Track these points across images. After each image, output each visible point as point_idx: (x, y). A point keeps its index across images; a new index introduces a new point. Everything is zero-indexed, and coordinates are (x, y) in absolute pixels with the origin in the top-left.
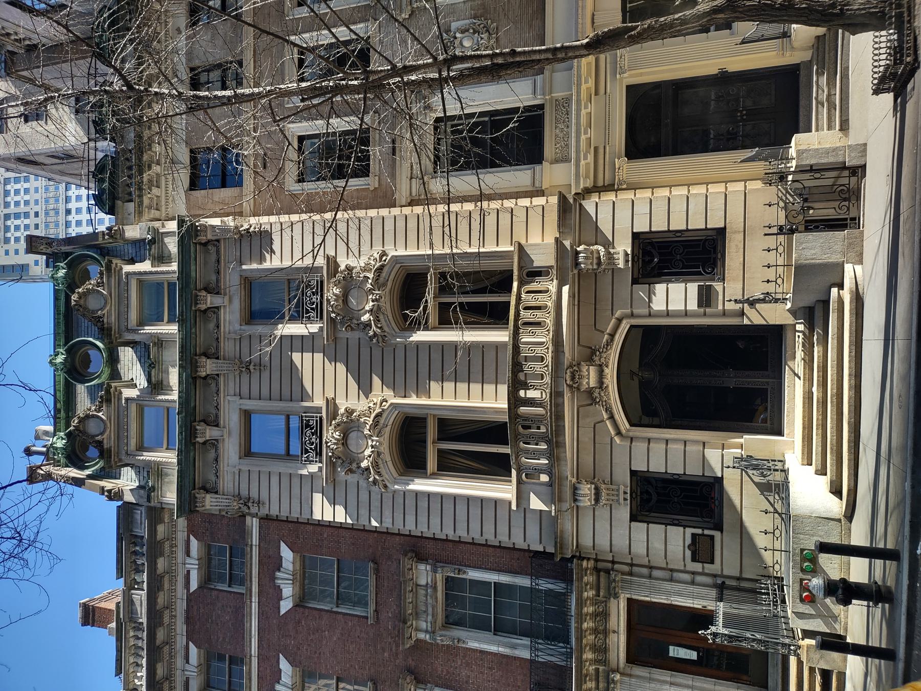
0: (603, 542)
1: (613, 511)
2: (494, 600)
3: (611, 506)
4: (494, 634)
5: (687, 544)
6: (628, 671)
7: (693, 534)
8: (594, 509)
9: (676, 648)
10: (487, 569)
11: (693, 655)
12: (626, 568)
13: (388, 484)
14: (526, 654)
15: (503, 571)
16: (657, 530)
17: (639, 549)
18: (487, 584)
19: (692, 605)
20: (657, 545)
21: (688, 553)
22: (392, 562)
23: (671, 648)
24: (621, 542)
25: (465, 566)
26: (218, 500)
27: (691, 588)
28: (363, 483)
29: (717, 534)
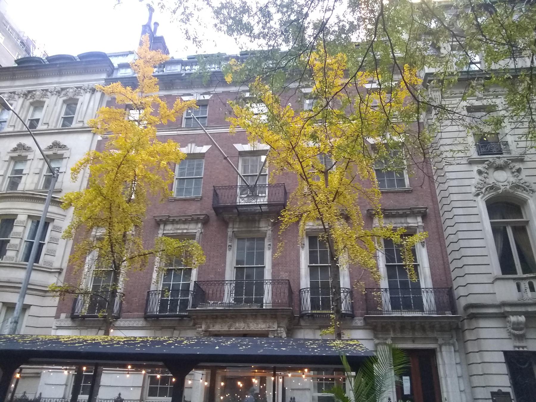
0: (483, 333)
5: (500, 388)
8: (506, 327)
9: (409, 381)
10: (429, 259)
11: (407, 391)
12: (457, 348)
13: (480, 197)
16: (504, 369)
17: (488, 357)
20: (494, 369)
21: (495, 390)
22: (415, 201)
23: (408, 378)
24: (487, 345)
25: (427, 246)
26: (438, 96)
28: (474, 182)
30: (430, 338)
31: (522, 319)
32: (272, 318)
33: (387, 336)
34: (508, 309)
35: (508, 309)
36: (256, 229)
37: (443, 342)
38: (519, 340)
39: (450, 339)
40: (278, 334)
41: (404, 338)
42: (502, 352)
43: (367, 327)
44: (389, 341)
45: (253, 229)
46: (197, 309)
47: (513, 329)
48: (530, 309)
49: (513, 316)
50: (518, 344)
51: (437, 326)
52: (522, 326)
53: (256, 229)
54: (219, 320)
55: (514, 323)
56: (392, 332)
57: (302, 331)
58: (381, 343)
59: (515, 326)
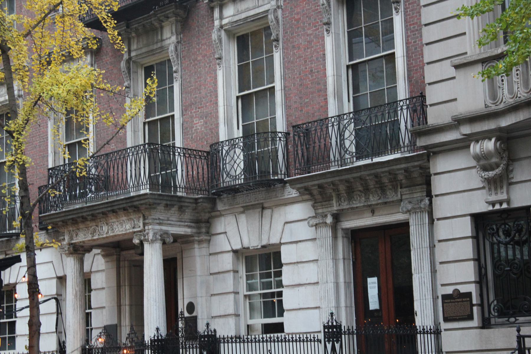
1: (479, 192)
2: (381, 57)
3: (483, 188)
4: (348, 67)
5: (458, 287)
6: (340, 234)
7: (470, 294)
9: (376, 285)
10: (407, 37)
11: (374, 304)
14: (332, 111)
15: (408, 61)
18: (390, 42)
19: (415, 299)
21: (449, 290)
23: (375, 279)
25: (405, 9)
27: (429, 297)
29: (476, 322)
30: (393, 202)
31: (490, 145)
32: (134, 211)
33: (330, 209)
34: (466, 130)
35: (466, 130)
36: (159, 45)
37: (410, 207)
38: (496, 189)
39: (421, 201)
40: (145, 236)
41: (352, 208)
42: (469, 217)
43: (307, 197)
44: (329, 220)
45: (155, 47)
46: (64, 210)
47: (485, 169)
48: (505, 122)
49: (477, 141)
50: (493, 198)
51: (400, 177)
52: (494, 160)
53: (159, 45)
54: (81, 226)
55: (477, 158)
56: (334, 202)
57: (223, 219)
58: (319, 223)
59: (482, 162)
